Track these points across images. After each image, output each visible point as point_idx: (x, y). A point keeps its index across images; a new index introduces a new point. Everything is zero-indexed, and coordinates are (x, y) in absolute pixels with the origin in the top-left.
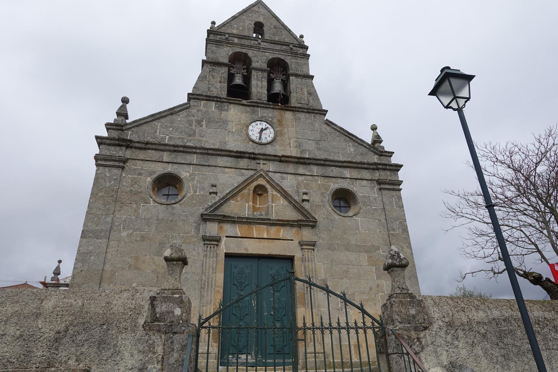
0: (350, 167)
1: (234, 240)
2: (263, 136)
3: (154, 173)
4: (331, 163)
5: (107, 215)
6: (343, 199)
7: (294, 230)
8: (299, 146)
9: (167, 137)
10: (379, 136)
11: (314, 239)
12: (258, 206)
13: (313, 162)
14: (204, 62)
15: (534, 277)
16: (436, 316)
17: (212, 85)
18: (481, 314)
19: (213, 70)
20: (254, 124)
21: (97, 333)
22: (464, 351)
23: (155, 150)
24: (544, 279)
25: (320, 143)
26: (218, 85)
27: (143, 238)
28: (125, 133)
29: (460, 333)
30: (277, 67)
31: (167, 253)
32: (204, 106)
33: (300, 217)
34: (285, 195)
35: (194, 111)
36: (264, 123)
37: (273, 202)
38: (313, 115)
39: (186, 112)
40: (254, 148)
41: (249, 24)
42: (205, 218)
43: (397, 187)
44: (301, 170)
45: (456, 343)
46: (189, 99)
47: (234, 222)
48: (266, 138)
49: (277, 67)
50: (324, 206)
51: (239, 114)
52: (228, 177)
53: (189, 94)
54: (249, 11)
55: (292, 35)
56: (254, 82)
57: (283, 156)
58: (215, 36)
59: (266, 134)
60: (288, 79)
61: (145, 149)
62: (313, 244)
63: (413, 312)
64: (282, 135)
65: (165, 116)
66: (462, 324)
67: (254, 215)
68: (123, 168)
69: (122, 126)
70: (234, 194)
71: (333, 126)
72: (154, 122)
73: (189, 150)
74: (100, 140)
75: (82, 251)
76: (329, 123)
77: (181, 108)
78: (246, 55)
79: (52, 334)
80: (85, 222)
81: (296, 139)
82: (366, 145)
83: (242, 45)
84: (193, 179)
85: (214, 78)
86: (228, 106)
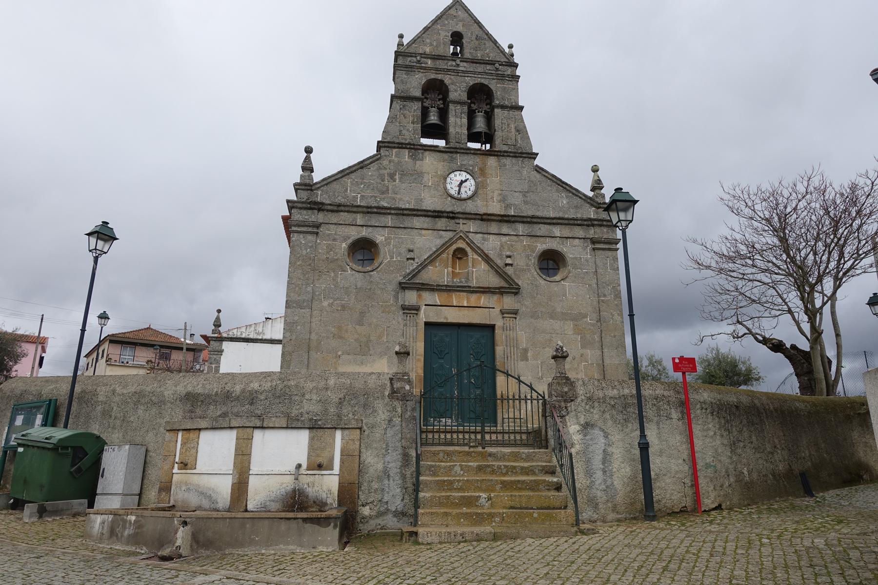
0: (561, 224)
1: (435, 309)
2: (463, 190)
4: (539, 220)
6: (551, 262)
7: (496, 297)
8: (503, 199)
10: (600, 180)
11: (516, 306)
12: (457, 271)
13: (519, 219)
14: (393, 98)
15: (773, 344)
17: (404, 127)
18: (615, 392)
19: (404, 106)
20: (452, 175)
21: (362, 399)
23: (348, 212)
24: (788, 346)
25: (528, 195)
26: (411, 127)
27: (344, 307)
29: (596, 404)
30: (480, 95)
31: (397, 349)
33: (503, 284)
34: (487, 259)
35: (385, 162)
36: (464, 174)
37: (473, 267)
41: (445, 35)
42: (403, 287)
43: (613, 246)
44: (505, 229)
46: (379, 148)
47: (432, 290)
49: (480, 95)
50: (529, 270)
52: (425, 240)
53: (378, 142)
56: (452, 120)
57: (485, 214)
58: (405, 59)
59: (466, 187)
61: (337, 211)
62: (515, 312)
63: (566, 389)
67: (453, 282)
68: (317, 233)
70: (432, 260)
72: (344, 179)
74: (291, 204)
76: (539, 170)
78: (442, 81)
83: (437, 70)
84: (389, 244)
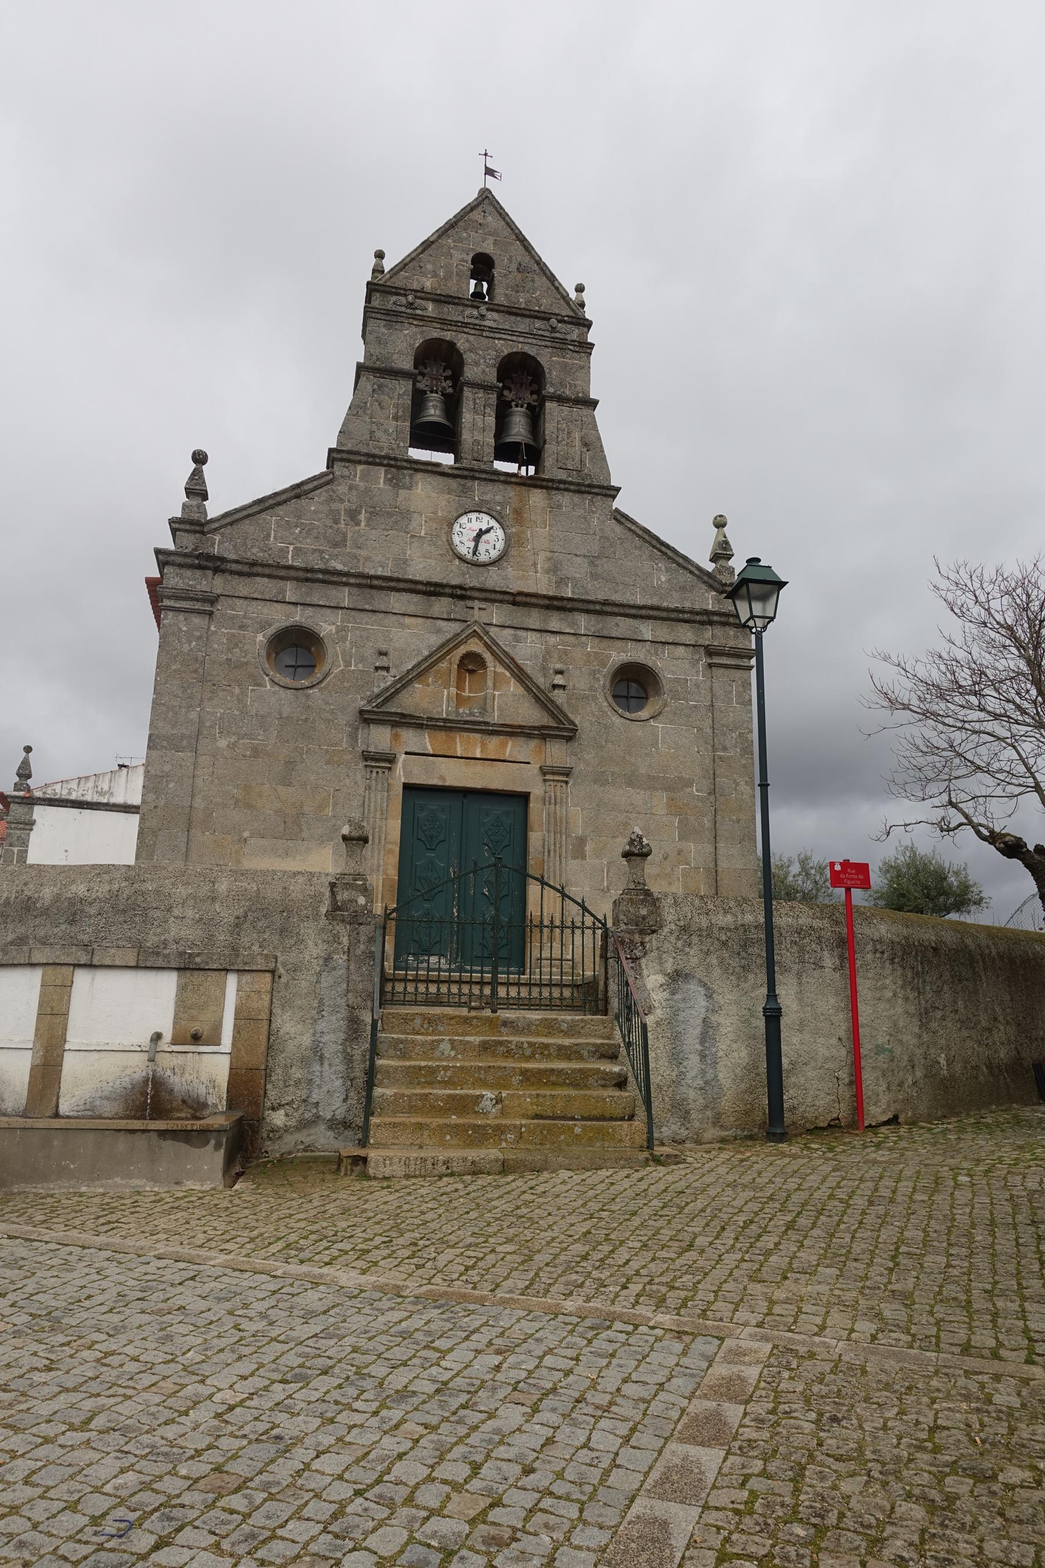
0: (655, 618)
1: (422, 759)
2: (482, 547)
3: (270, 625)
4: (616, 610)
5: (190, 707)
6: (634, 684)
7: (533, 744)
8: (554, 568)
9: (291, 548)
10: (727, 543)
11: (569, 762)
12: (466, 694)
13: (580, 606)
14: (360, 369)
15: (1005, 843)
16: (670, 918)
17: (379, 425)
18: (729, 918)
19: (380, 386)
20: (463, 520)
21: (277, 919)
22: (696, 959)
23: (269, 576)
24: (1031, 848)
25: (598, 562)
26: (391, 425)
27: (256, 752)
28: (208, 540)
29: (695, 939)
30: (520, 374)
31: (346, 830)
32: (363, 477)
33: (546, 720)
34: (520, 675)
35: (342, 489)
36: (486, 518)
37: (495, 688)
38: (589, 497)
39: (327, 491)
40: (464, 574)
41: (461, 259)
42: (367, 718)
43: (744, 662)
44: (555, 622)
45: (687, 949)
46: (331, 461)
47: (420, 726)
48: (487, 551)
49: (520, 374)
50: (595, 698)
51: (434, 495)
52: (410, 635)
53: (331, 451)
54: (461, 224)
55: (557, 288)
56: (467, 417)
57: (520, 594)
58: (387, 296)
59: (487, 542)
60: (542, 405)
61: (249, 575)
62: (567, 772)
63: (644, 912)
64: (520, 543)
65: (285, 501)
66: (700, 929)
67: (458, 714)
68: (211, 614)
69: (202, 525)
70: (420, 672)
71: (629, 525)
72: (264, 515)
73: (335, 579)
74: (163, 557)
75: (152, 772)
76: (621, 518)
77: (315, 483)
78: (452, 345)
79: (232, 919)
80: (152, 721)
81: (548, 554)
82: (693, 569)
83: (444, 323)
84: (344, 639)
85: (382, 408)
86: (411, 476)
